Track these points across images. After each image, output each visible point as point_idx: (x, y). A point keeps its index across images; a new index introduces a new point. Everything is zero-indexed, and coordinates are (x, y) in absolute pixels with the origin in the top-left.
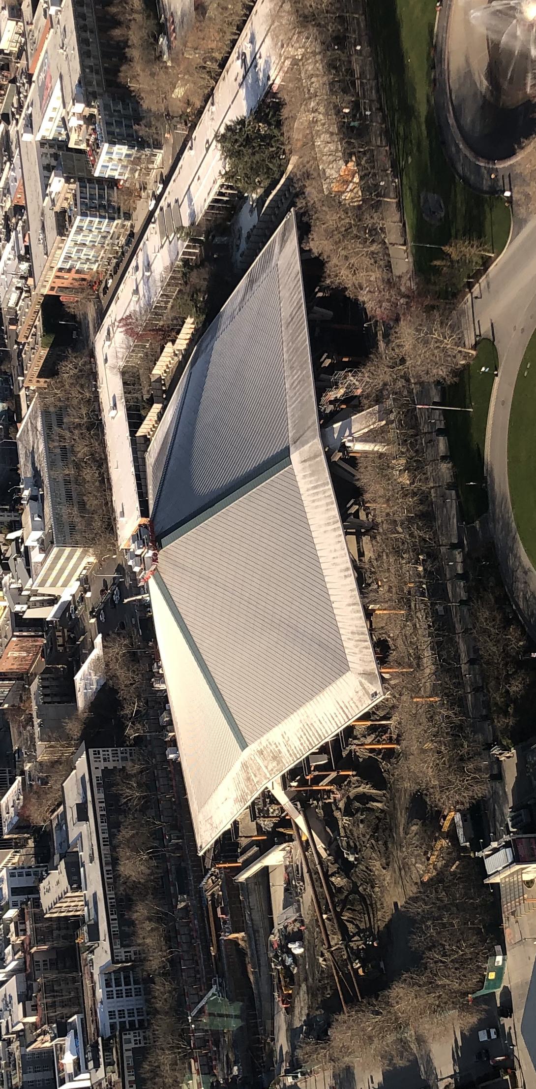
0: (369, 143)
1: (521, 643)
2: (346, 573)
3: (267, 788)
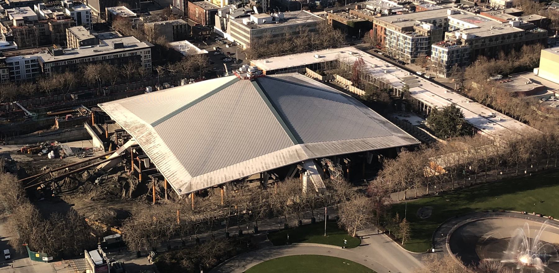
0: (455, 179)
1: (208, 265)
2: (241, 174)
3: (132, 137)
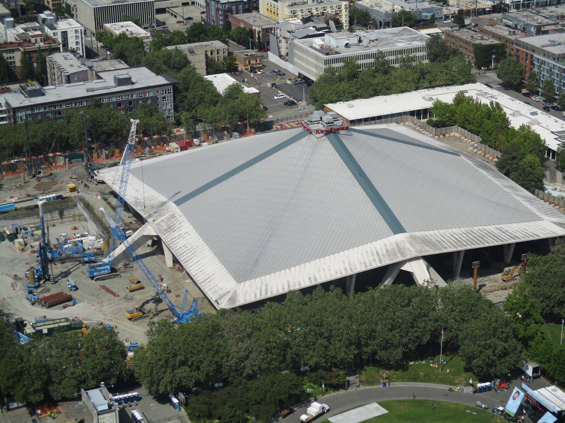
2: (313, 279)
